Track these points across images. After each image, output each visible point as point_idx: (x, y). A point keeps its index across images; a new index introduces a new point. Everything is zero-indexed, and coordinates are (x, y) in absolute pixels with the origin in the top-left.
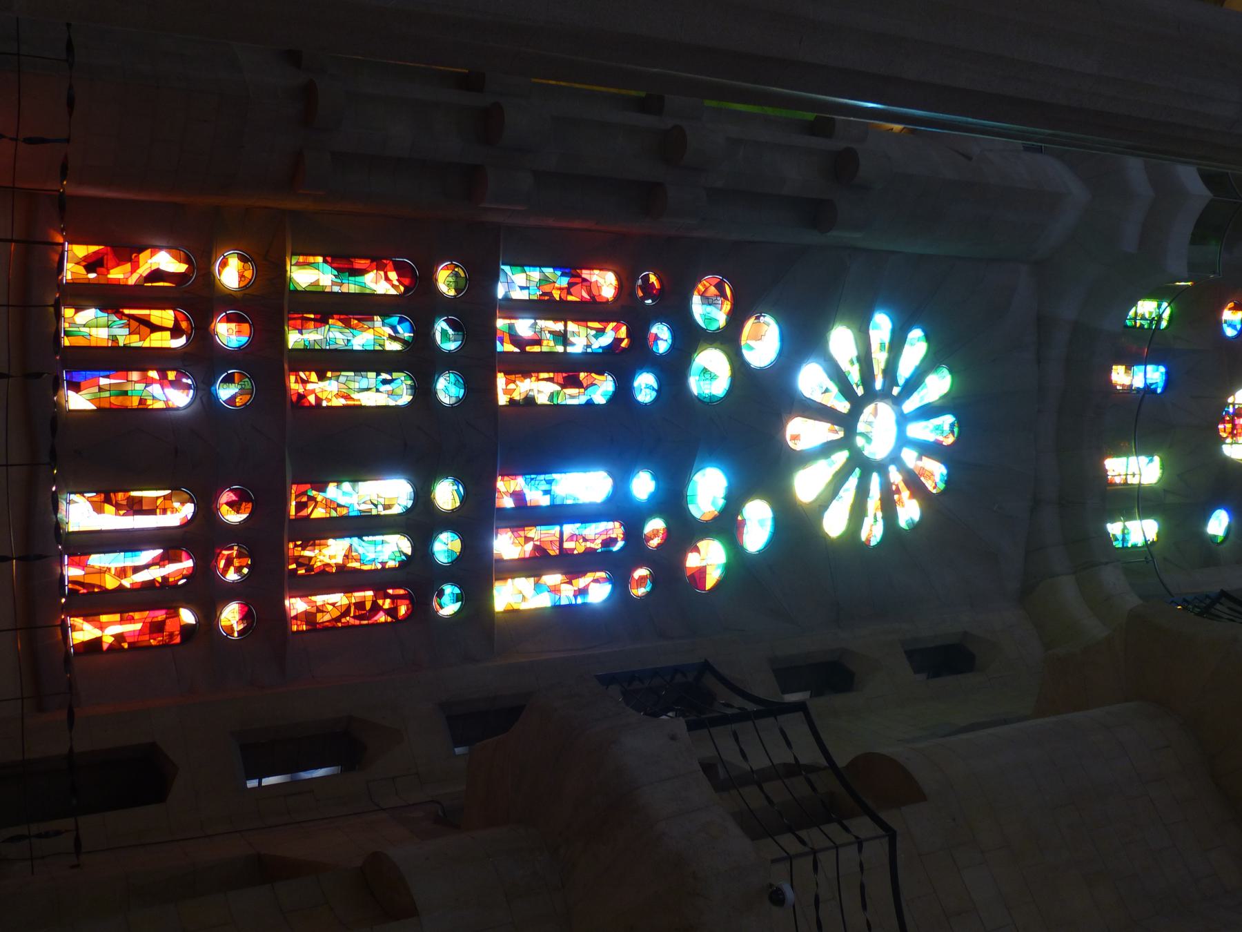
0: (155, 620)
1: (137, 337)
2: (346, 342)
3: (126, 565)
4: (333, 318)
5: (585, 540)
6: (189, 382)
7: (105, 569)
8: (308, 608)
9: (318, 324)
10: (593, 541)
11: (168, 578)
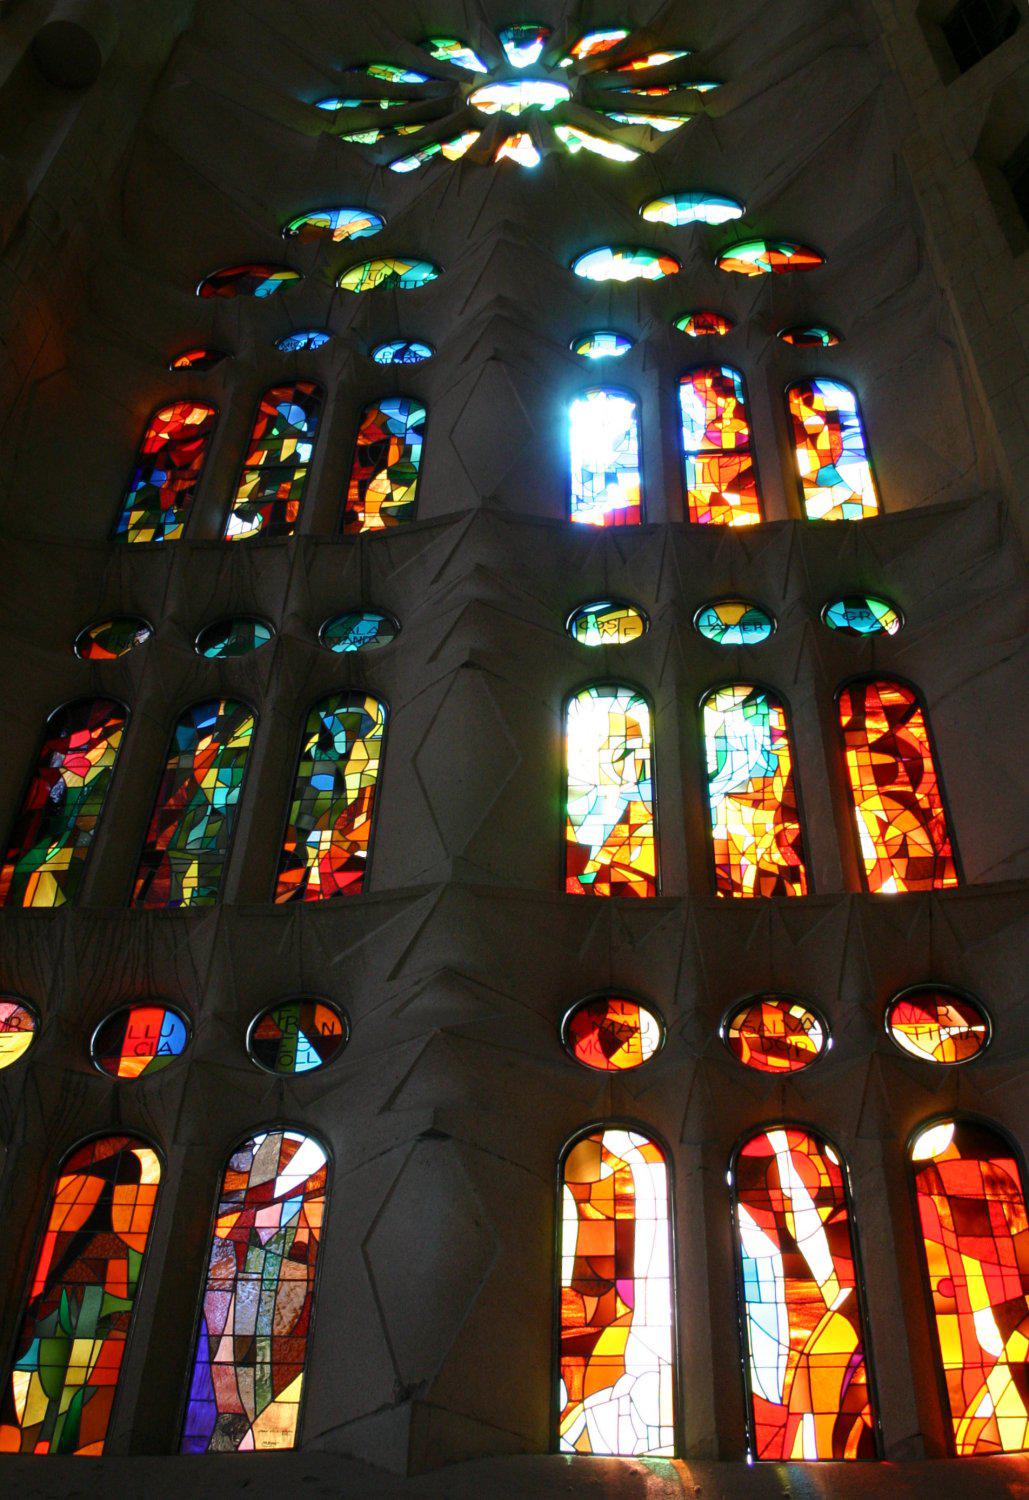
0: (948, 1222)
1: (115, 1267)
2: (215, 818)
3: (781, 1298)
4: (154, 844)
5: (719, 419)
7: (795, 1355)
8: (896, 875)
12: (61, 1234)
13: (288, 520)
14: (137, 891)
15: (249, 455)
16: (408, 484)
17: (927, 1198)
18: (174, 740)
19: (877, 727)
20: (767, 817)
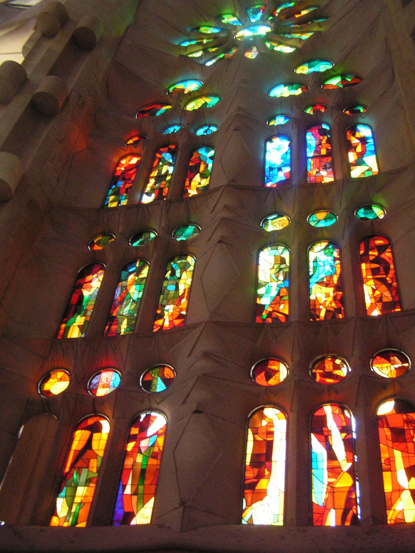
0: (390, 438)
2: (133, 303)
4: (112, 313)
6: (143, 416)
7: (329, 488)
8: (377, 308)
9: (114, 322)
10: (321, 141)
11: (342, 427)
12: (75, 450)
13: (164, 195)
14: (106, 330)
15: (151, 173)
16: (206, 178)
17: (382, 429)
18: (120, 276)
19: (374, 253)
20: (330, 290)
